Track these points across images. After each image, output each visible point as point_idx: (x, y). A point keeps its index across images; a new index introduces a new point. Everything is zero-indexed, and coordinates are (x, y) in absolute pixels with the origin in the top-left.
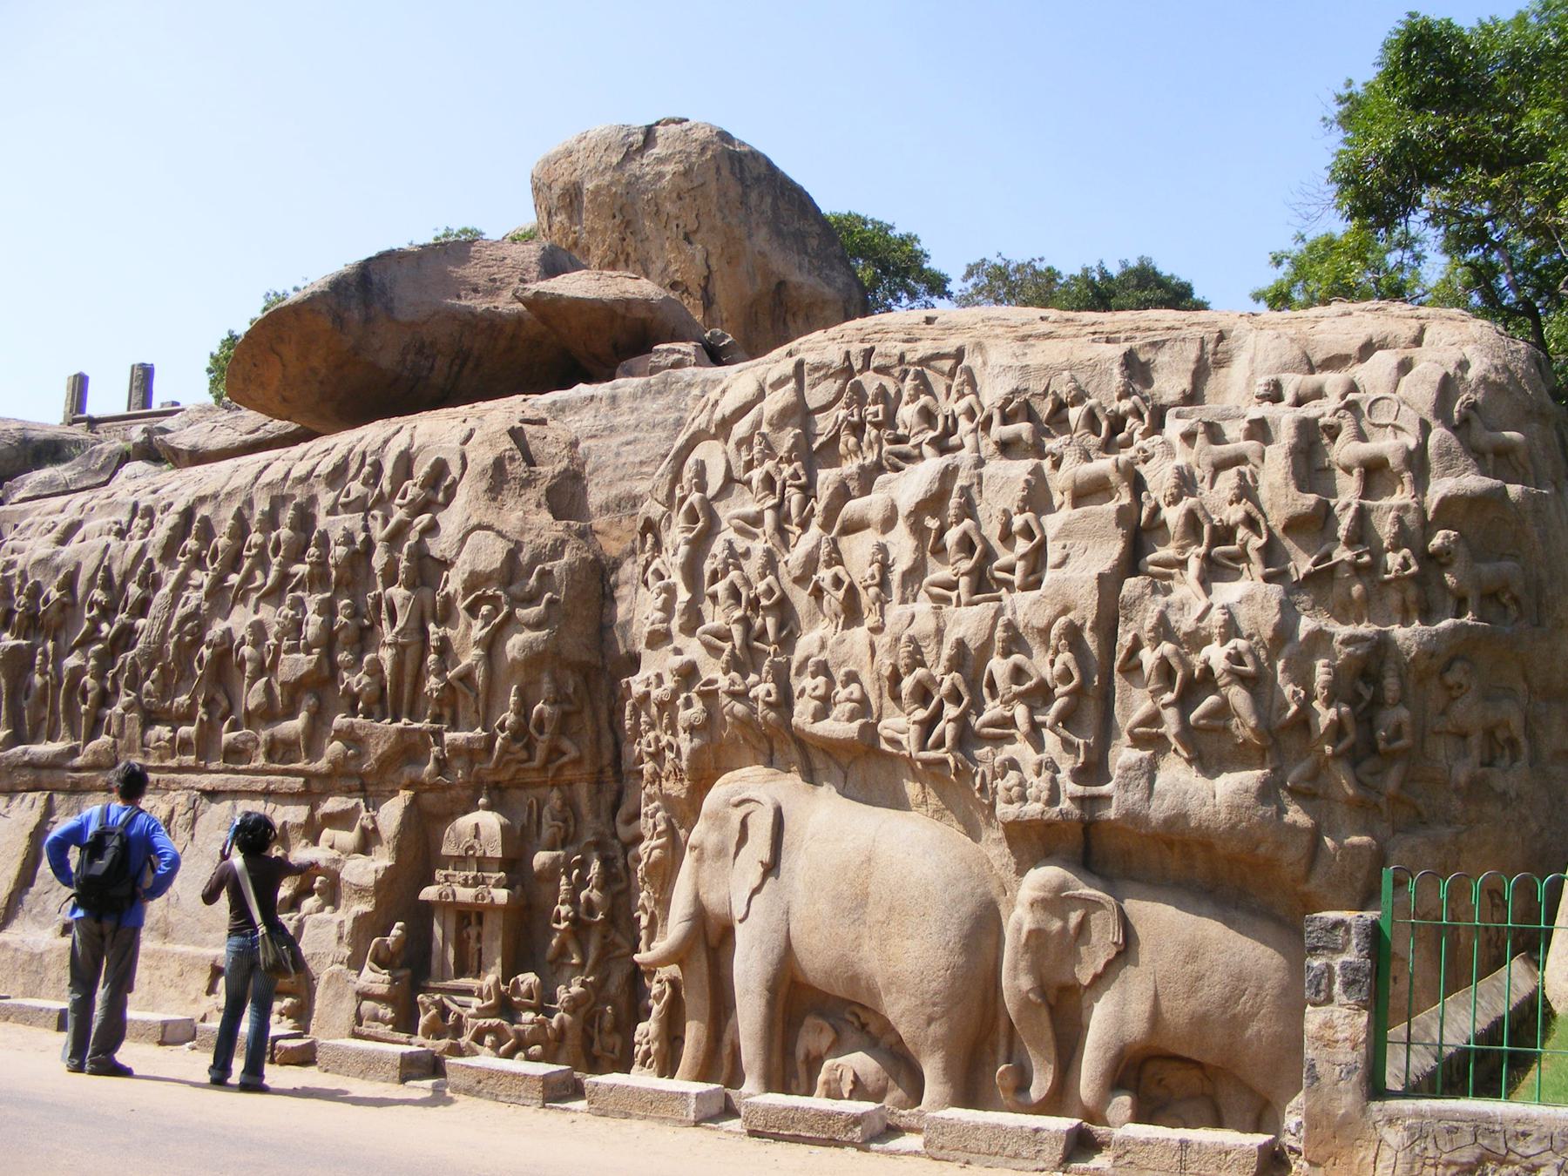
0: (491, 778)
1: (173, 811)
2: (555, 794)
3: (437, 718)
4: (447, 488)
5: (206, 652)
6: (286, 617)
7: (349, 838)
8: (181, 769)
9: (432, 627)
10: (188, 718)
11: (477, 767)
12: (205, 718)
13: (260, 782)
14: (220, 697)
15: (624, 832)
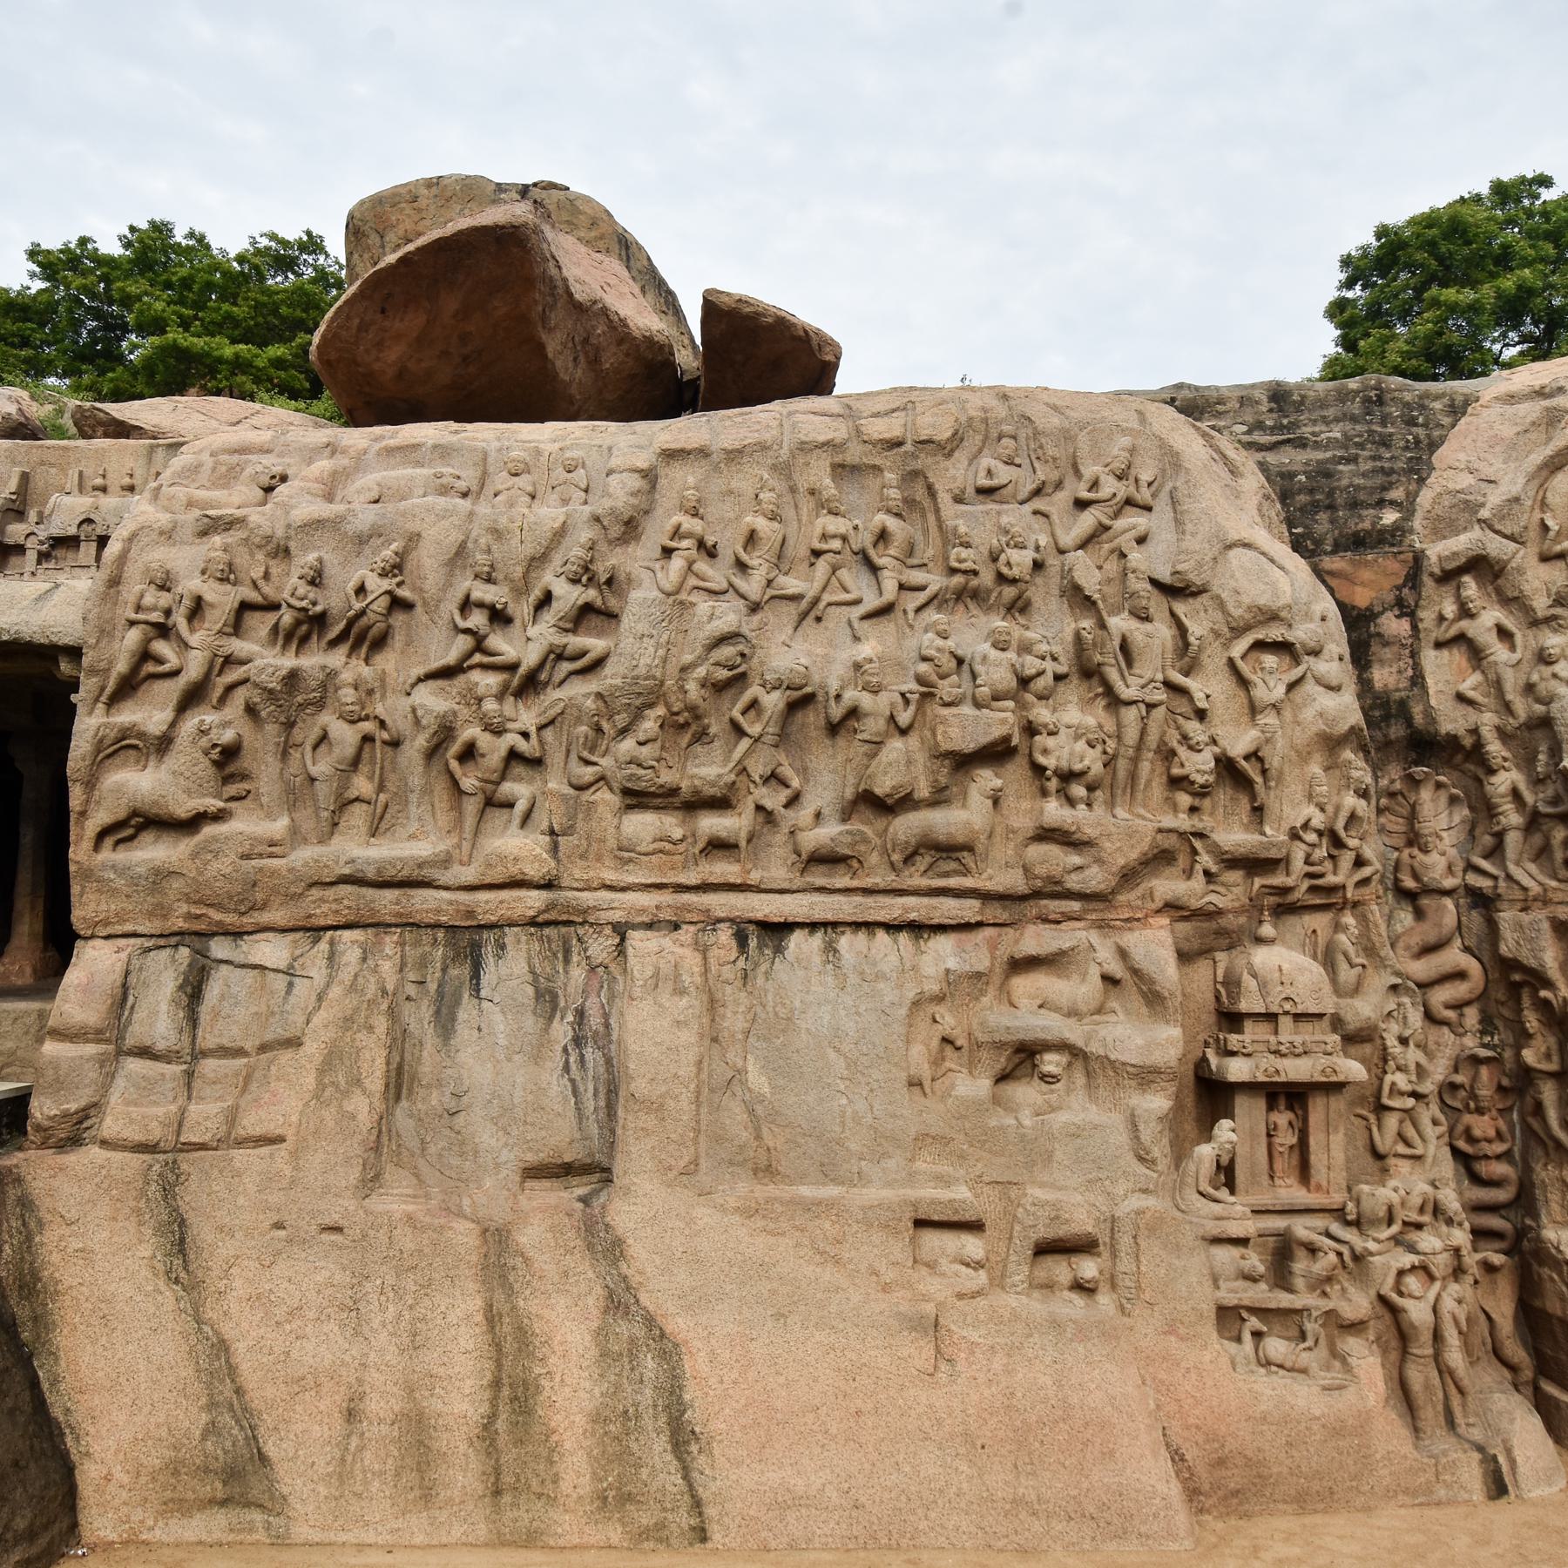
0: (1273, 900)
1: (705, 958)
2: (1349, 919)
3: (1193, 810)
4: (1150, 484)
5: (773, 701)
6: (939, 650)
7: (1081, 988)
8: (704, 887)
9: (1178, 678)
10: (721, 803)
11: (1258, 882)
12: (768, 804)
13: (892, 908)
14: (787, 771)
15: (1421, 969)
